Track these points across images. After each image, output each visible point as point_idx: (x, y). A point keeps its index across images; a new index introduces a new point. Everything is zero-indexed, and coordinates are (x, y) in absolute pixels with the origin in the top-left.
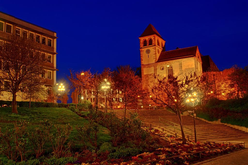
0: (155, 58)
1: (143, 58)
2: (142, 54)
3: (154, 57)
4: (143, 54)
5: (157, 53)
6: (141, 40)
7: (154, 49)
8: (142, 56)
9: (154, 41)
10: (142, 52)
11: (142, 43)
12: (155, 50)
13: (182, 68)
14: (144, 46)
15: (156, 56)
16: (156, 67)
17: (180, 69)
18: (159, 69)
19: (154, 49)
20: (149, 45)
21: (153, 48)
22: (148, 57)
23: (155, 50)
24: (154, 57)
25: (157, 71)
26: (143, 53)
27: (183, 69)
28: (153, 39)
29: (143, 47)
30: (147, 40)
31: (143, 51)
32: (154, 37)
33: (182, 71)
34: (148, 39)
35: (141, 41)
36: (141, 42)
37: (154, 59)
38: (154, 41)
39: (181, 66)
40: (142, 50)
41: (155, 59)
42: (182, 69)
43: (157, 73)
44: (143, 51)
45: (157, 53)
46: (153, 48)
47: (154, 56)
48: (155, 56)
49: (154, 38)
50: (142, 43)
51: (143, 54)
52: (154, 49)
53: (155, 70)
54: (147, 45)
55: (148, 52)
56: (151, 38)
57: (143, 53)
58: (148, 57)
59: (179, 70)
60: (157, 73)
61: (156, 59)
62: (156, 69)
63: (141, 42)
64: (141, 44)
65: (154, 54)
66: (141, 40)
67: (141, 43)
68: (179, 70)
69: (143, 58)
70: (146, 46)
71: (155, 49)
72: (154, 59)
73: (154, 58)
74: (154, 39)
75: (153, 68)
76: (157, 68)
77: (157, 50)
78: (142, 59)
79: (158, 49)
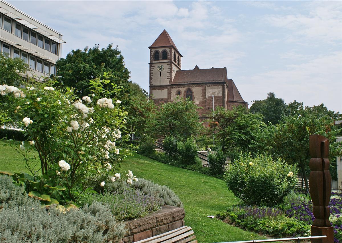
0: (170, 77)
1: (152, 76)
3: (168, 76)
6: (152, 51)
9: (169, 54)
10: (152, 68)
11: (152, 56)
12: (170, 67)
13: (205, 95)
14: (155, 60)
15: (171, 76)
17: (202, 96)
18: (174, 94)
19: (170, 65)
20: (163, 59)
21: (168, 64)
22: (160, 76)
23: (170, 67)
24: (168, 76)
25: (171, 96)
26: (153, 69)
27: (207, 96)
28: (169, 52)
29: (154, 62)
30: (160, 52)
32: (170, 50)
33: (205, 100)
35: (152, 52)
37: (168, 79)
38: (169, 54)
39: (205, 93)
40: (153, 66)
41: (169, 80)
43: (171, 99)
44: (154, 66)
48: (170, 75)
50: (152, 56)
52: (170, 65)
53: (169, 94)
54: (160, 58)
56: (166, 50)
57: (153, 69)
58: (160, 76)
60: (172, 98)
62: (171, 93)
63: (152, 54)
65: (169, 72)
66: (152, 51)
67: (152, 55)
69: (152, 76)
70: (158, 60)
72: (168, 79)
73: (168, 77)
74: (171, 51)
75: (165, 91)
76: (172, 91)
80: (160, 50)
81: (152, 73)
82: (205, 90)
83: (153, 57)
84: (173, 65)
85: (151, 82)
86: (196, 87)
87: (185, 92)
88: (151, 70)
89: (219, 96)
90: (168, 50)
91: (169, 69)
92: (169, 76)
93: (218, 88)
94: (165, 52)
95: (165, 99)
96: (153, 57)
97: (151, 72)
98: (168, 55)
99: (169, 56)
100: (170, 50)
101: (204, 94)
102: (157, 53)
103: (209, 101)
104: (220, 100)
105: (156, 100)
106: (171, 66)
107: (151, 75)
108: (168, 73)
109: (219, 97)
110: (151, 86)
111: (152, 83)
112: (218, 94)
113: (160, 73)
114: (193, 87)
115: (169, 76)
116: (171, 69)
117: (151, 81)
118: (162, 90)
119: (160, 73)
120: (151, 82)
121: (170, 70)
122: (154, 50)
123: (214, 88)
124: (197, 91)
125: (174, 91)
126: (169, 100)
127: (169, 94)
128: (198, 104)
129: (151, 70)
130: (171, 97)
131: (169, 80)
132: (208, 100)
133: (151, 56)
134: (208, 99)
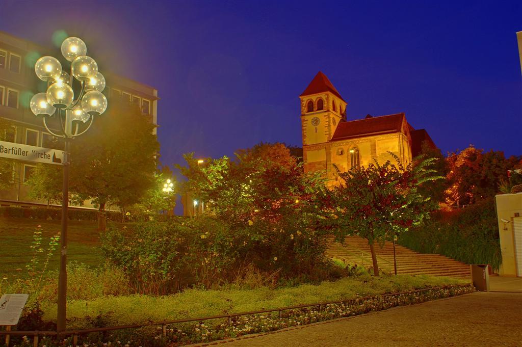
0: (328, 133)
2: (304, 125)
5: (332, 124)
8: (305, 129)
9: (326, 103)
10: (305, 122)
11: (305, 107)
12: (327, 120)
13: (376, 152)
14: (308, 111)
15: (330, 130)
16: (330, 149)
21: (325, 116)
23: (327, 120)
26: (306, 123)
28: (325, 100)
29: (306, 114)
30: (314, 100)
31: (307, 120)
32: (326, 96)
34: (316, 99)
35: (303, 102)
38: (326, 103)
39: (375, 149)
43: (330, 161)
44: (307, 120)
45: (332, 124)
46: (325, 116)
47: (326, 129)
50: (305, 107)
53: (328, 154)
54: (314, 109)
55: (316, 121)
57: (306, 123)
59: (371, 156)
60: (332, 160)
61: (330, 135)
64: (303, 108)
68: (371, 156)
70: (313, 111)
71: (329, 117)
73: (326, 133)
74: (327, 99)
75: (323, 151)
76: (331, 151)
77: (331, 119)
78: (305, 134)
79: (333, 119)
99: (325, 105)
101: (374, 149)
130: (330, 158)
131: (328, 136)
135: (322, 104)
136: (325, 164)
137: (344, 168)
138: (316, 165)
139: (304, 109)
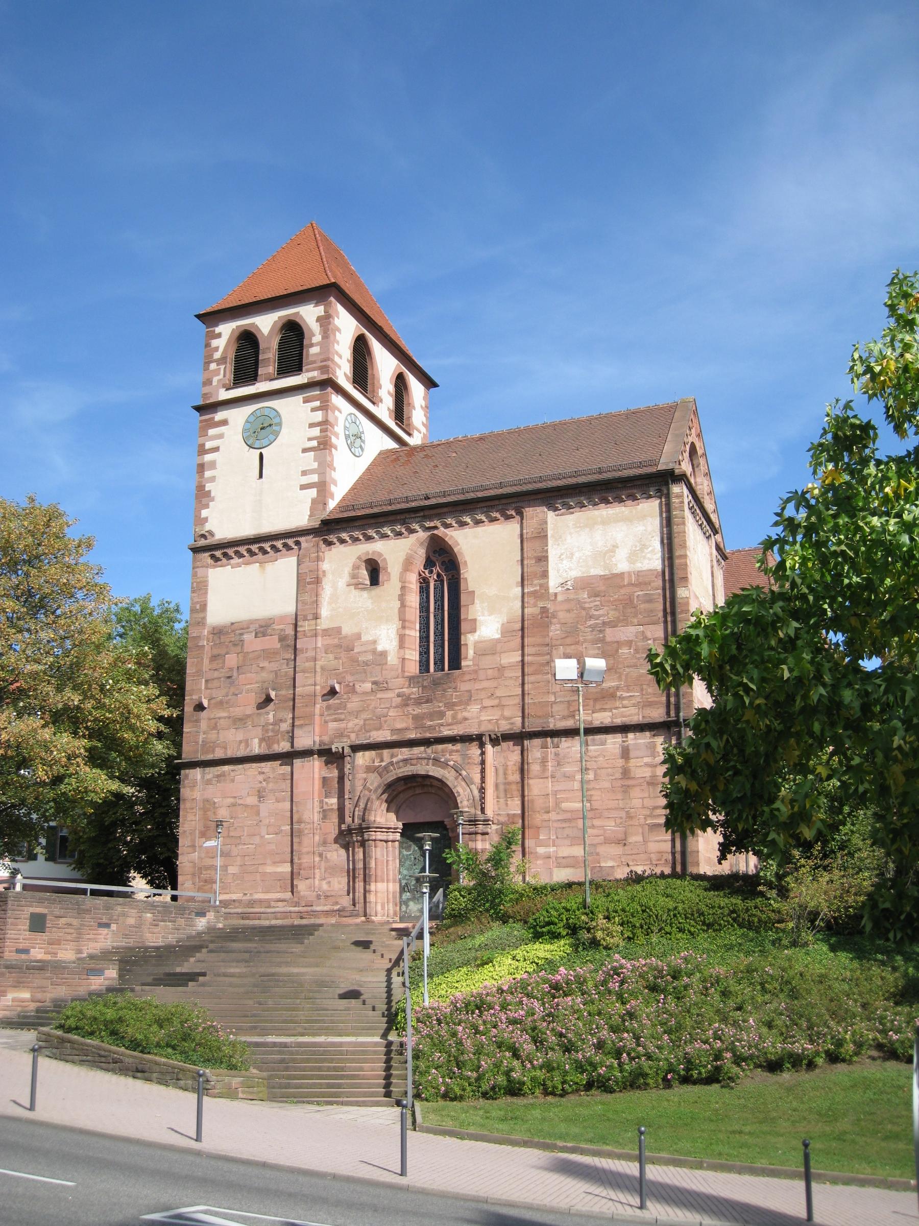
3: (304, 473)
4: (216, 449)
7: (313, 410)
8: (213, 465)
9: (317, 338)
10: (212, 432)
12: (318, 416)
13: (545, 574)
16: (318, 559)
19: (317, 403)
21: (306, 401)
22: (261, 476)
23: (318, 416)
24: (304, 473)
26: (221, 436)
27: (553, 583)
29: (224, 395)
35: (215, 343)
36: (217, 349)
37: (303, 487)
38: (317, 338)
39: (543, 559)
41: (313, 493)
42: (545, 587)
43: (316, 617)
44: (224, 422)
49: (319, 319)
51: (216, 449)
52: (317, 403)
53: (309, 582)
54: (261, 371)
57: (221, 436)
58: (261, 476)
60: (324, 612)
61: (322, 487)
62: (318, 581)
63: (217, 349)
65: (314, 443)
66: (219, 336)
67: (217, 355)
69: (213, 479)
72: (303, 487)
74: (325, 321)
76: (325, 566)
80: (265, 324)
81: (213, 465)
82: (542, 536)
83: (222, 367)
84: (337, 400)
85: (206, 520)
86: (478, 522)
87: (408, 564)
88: (209, 445)
89: (639, 573)
90: (309, 314)
91: (312, 425)
92: (312, 472)
93: (628, 520)
94: (293, 332)
95: (282, 618)
96: (222, 367)
97: (208, 458)
98: (312, 345)
99: (314, 350)
100: (320, 310)
102: (248, 339)
103: (568, 611)
104: (650, 601)
105: (227, 633)
106: (325, 407)
107: (208, 474)
108: (305, 450)
109: (641, 580)
110: (202, 542)
111: (208, 527)
112: (633, 556)
113: (261, 456)
114: (462, 524)
115: (312, 472)
116: (325, 425)
117: (204, 513)
118: (269, 567)
119: (261, 456)
120: (206, 520)
121: (316, 431)
122: (227, 330)
123: (605, 522)
124: (486, 549)
125: (341, 560)
126: (305, 626)
127: (309, 582)
128: (497, 636)
129: (209, 445)
130: (316, 603)
131: (313, 493)
132: (566, 606)
133: (213, 366)
134: (568, 600)
135: (301, 346)
136: (290, 631)
137: (384, 654)
138: (248, 637)
139: (217, 372)
